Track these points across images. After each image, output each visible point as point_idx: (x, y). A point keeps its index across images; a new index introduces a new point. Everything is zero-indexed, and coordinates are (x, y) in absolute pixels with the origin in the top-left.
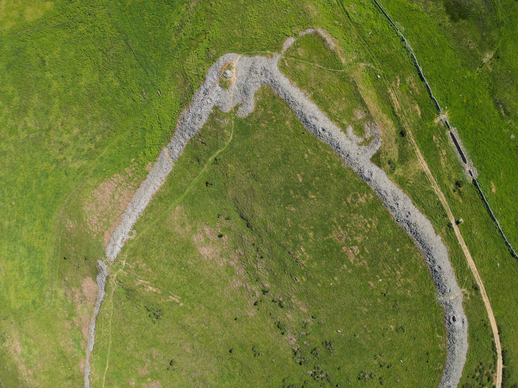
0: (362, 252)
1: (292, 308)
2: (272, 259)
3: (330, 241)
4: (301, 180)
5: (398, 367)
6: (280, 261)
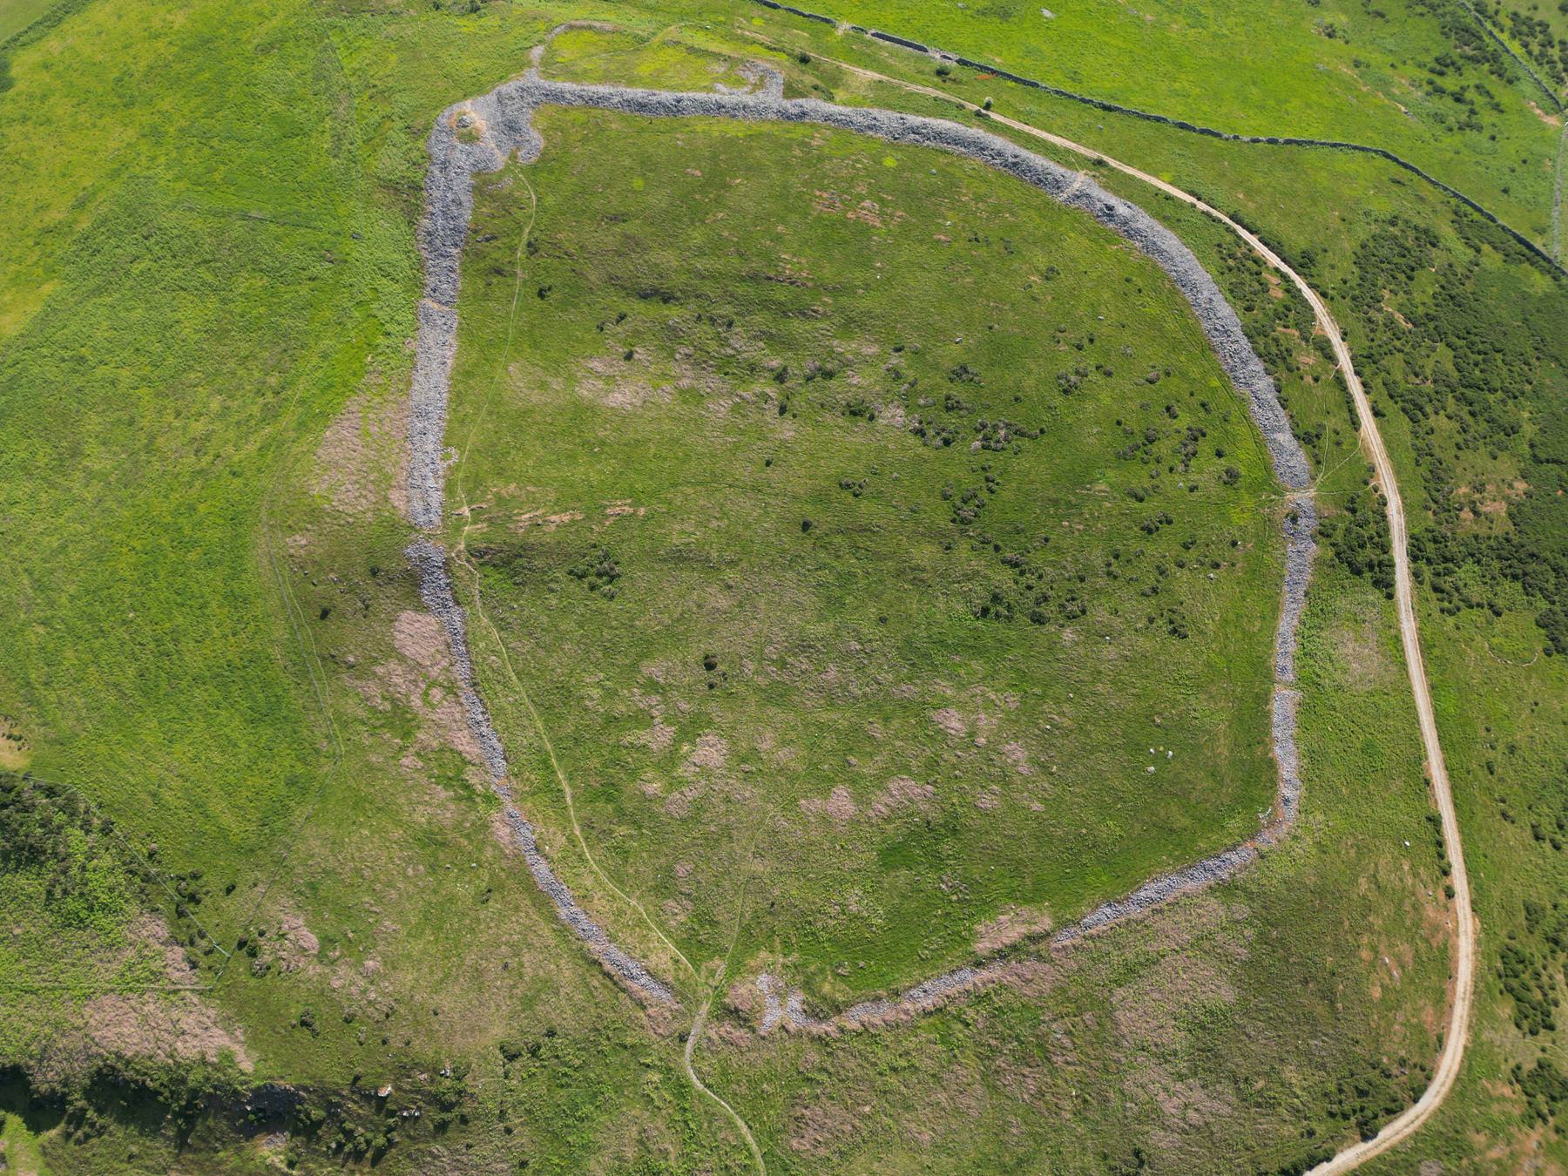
1: (848, 364)
2: (750, 312)
3: (819, 219)
4: (698, 173)
5: (1106, 331)
6: (765, 304)
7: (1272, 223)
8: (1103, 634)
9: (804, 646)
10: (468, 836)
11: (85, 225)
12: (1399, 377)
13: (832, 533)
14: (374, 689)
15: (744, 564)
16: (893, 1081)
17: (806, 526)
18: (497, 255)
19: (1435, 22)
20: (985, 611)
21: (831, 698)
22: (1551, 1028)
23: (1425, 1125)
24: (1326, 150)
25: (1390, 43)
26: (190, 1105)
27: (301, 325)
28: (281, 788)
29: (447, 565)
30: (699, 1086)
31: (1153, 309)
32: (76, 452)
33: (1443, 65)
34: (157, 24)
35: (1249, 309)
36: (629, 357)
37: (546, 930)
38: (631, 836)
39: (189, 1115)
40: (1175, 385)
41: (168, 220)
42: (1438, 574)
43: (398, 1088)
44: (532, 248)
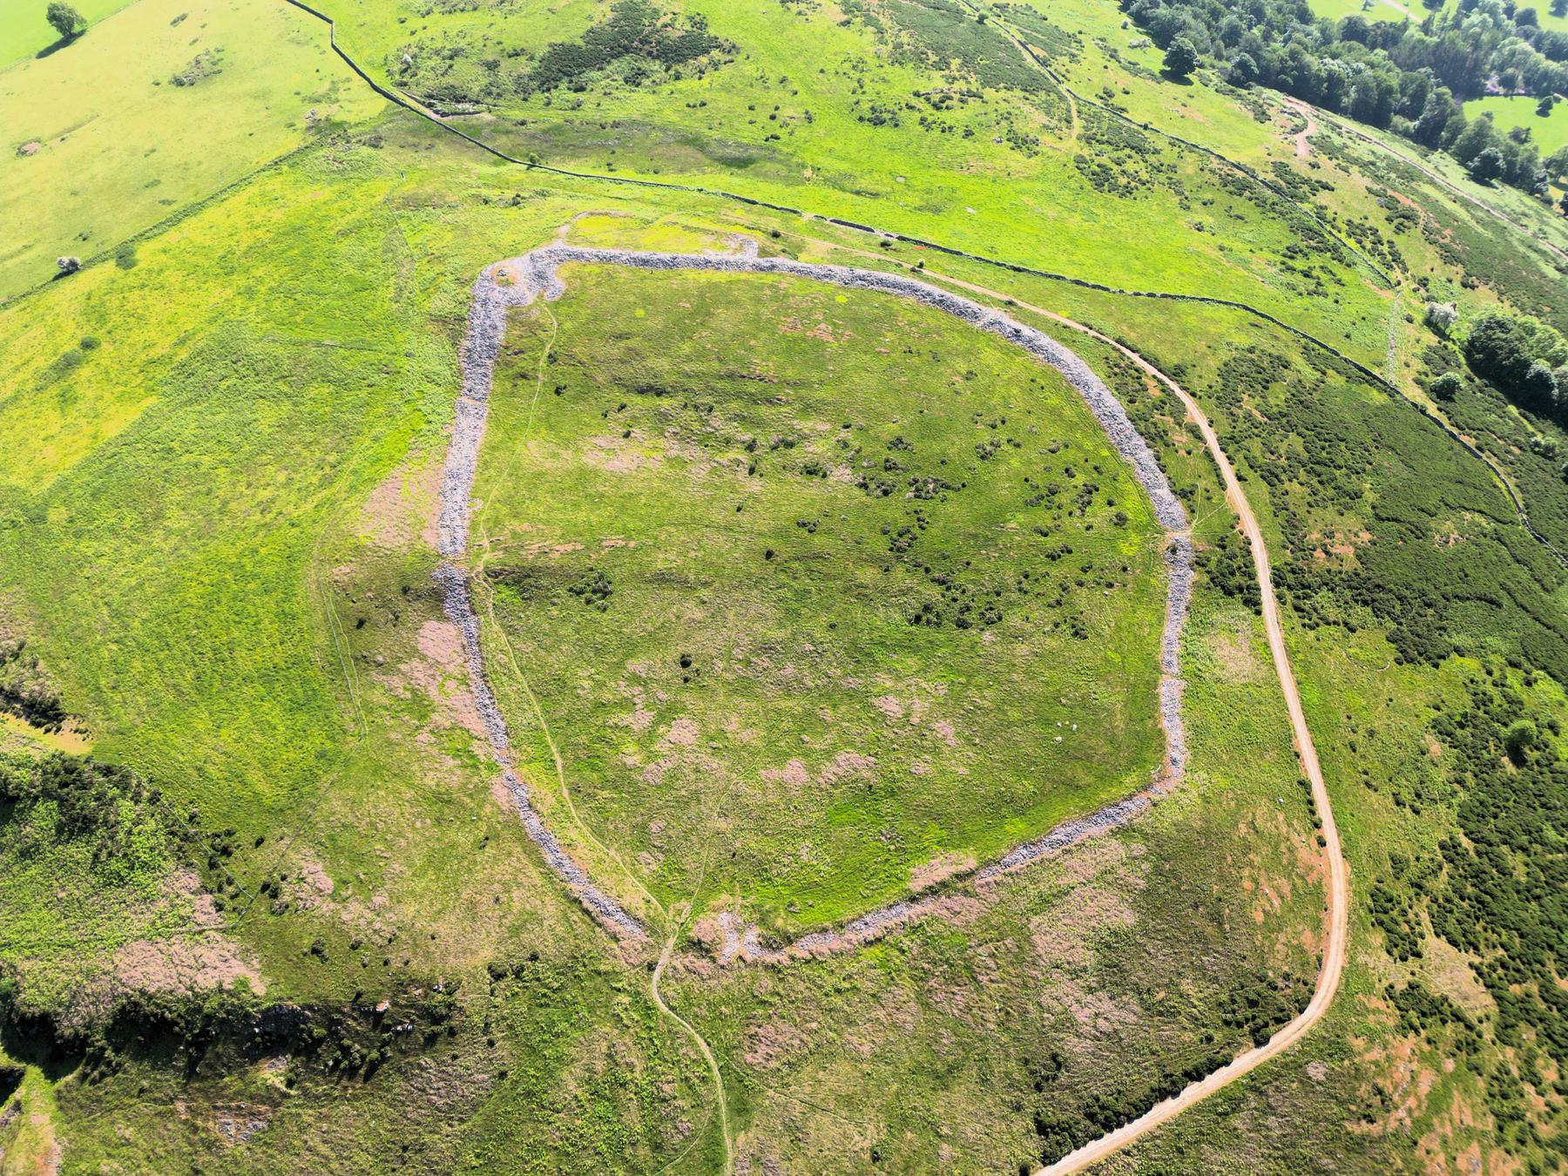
1: (806, 437)
3: (784, 336)
6: (738, 396)
7: (1151, 346)
8: (1019, 636)
9: (767, 648)
10: (471, 796)
11: (183, 355)
12: (1258, 454)
13: (792, 562)
14: (397, 682)
15: (716, 585)
16: (838, 1001)
17: (769, 554)
18: (523, 364)
19: (1285, 223)
20: (918, 619)
21: (788, 689)
22: (1418, 955)
23: (1310, 1031)
24: (1196, 302)
25: (1249, 236)
26: (204, 1032)
27: (359, 418)
28: (311, 761)
29: (467, 583)
30: (665, 1009)
31: (1054, 401)
32: (158, 516)
33: (1292, 252)
34: (258, 219)
35: (1132, 402)
36: (627, 435)
37: (534, 873)
38: (613, 799)
39: (201, 1043)
40: (1071, 455)
41: (255, 349)
42: (1298, 597)
43: (394, 1004)
44: (552, 359)
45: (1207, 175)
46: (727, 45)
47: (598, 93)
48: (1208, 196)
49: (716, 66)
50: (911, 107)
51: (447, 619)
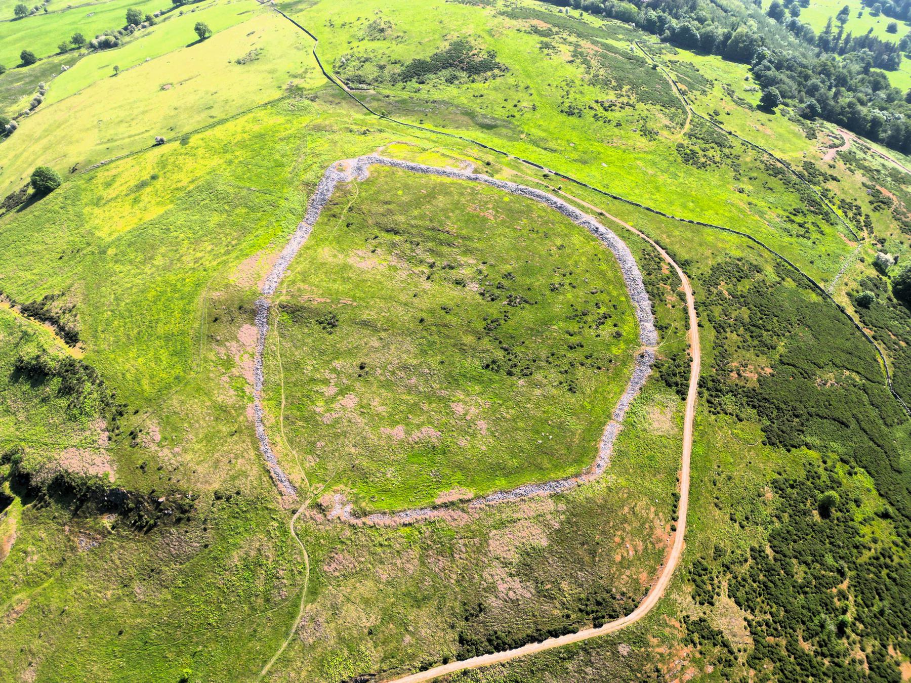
0: (497, 211)
1: (461, 265)
6: (434, 239)
7: (677, 248)
8: (538, 385)
9: (405, 368)
10: (236, 410)
11: (191, 187)
12: (717, 314)
13: (433, 327)
14: (223, 351)
16: (379, 550)
18: (336, 210)
19: (799, 196)
20: (488, 366)
21: (409, 390)
22: (712, 604)
23: (628, 627)
25: (772, 200)
26: (85, 495)
27: (252, 225)
28: (171, 380)
30: (293, 534)
31: (604, 267)
32: (151, 258)
33: (796, 212)
34: (247, 129)
36: (373, 251)
37: (252, 454)
38: (303, 427)
39: (83, 500)
40: (604, 297)
41: (220, 188)
42: (711, 395)
43: (167, 500)
44: (351, 209)
45: (758, 163)
46: (503, 67)
47: (431, 84)
48: (755, 175)
49: (494, 77)
50: (590, 108)
51: (255, 325)
